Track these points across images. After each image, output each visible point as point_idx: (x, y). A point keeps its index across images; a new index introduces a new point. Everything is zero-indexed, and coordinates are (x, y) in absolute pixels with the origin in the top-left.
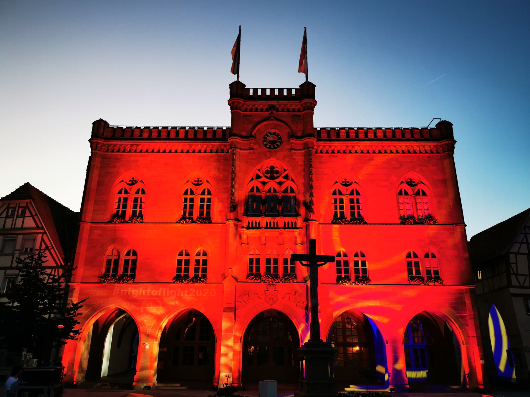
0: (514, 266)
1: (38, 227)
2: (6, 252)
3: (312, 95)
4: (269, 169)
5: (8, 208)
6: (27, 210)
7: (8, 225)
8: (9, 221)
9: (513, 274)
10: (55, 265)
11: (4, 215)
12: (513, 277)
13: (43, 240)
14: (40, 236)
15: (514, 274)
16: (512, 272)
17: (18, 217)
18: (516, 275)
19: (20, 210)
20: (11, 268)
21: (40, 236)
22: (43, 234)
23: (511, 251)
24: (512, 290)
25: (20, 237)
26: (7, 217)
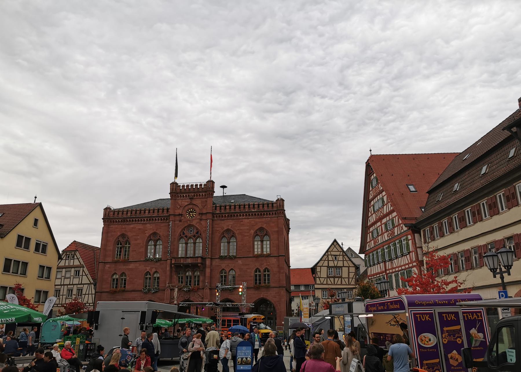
0: (319, 273)
2: (66, 276)
3: (213, 188)
5: (66, 255)
7: (67, 264)
8: (67, 261)
11: (64, 258)
12: (318, 279)
13: (83, 270)
18: (319, 278)
20: (70, 285)
24: (316, 286)
26: (66, 260)
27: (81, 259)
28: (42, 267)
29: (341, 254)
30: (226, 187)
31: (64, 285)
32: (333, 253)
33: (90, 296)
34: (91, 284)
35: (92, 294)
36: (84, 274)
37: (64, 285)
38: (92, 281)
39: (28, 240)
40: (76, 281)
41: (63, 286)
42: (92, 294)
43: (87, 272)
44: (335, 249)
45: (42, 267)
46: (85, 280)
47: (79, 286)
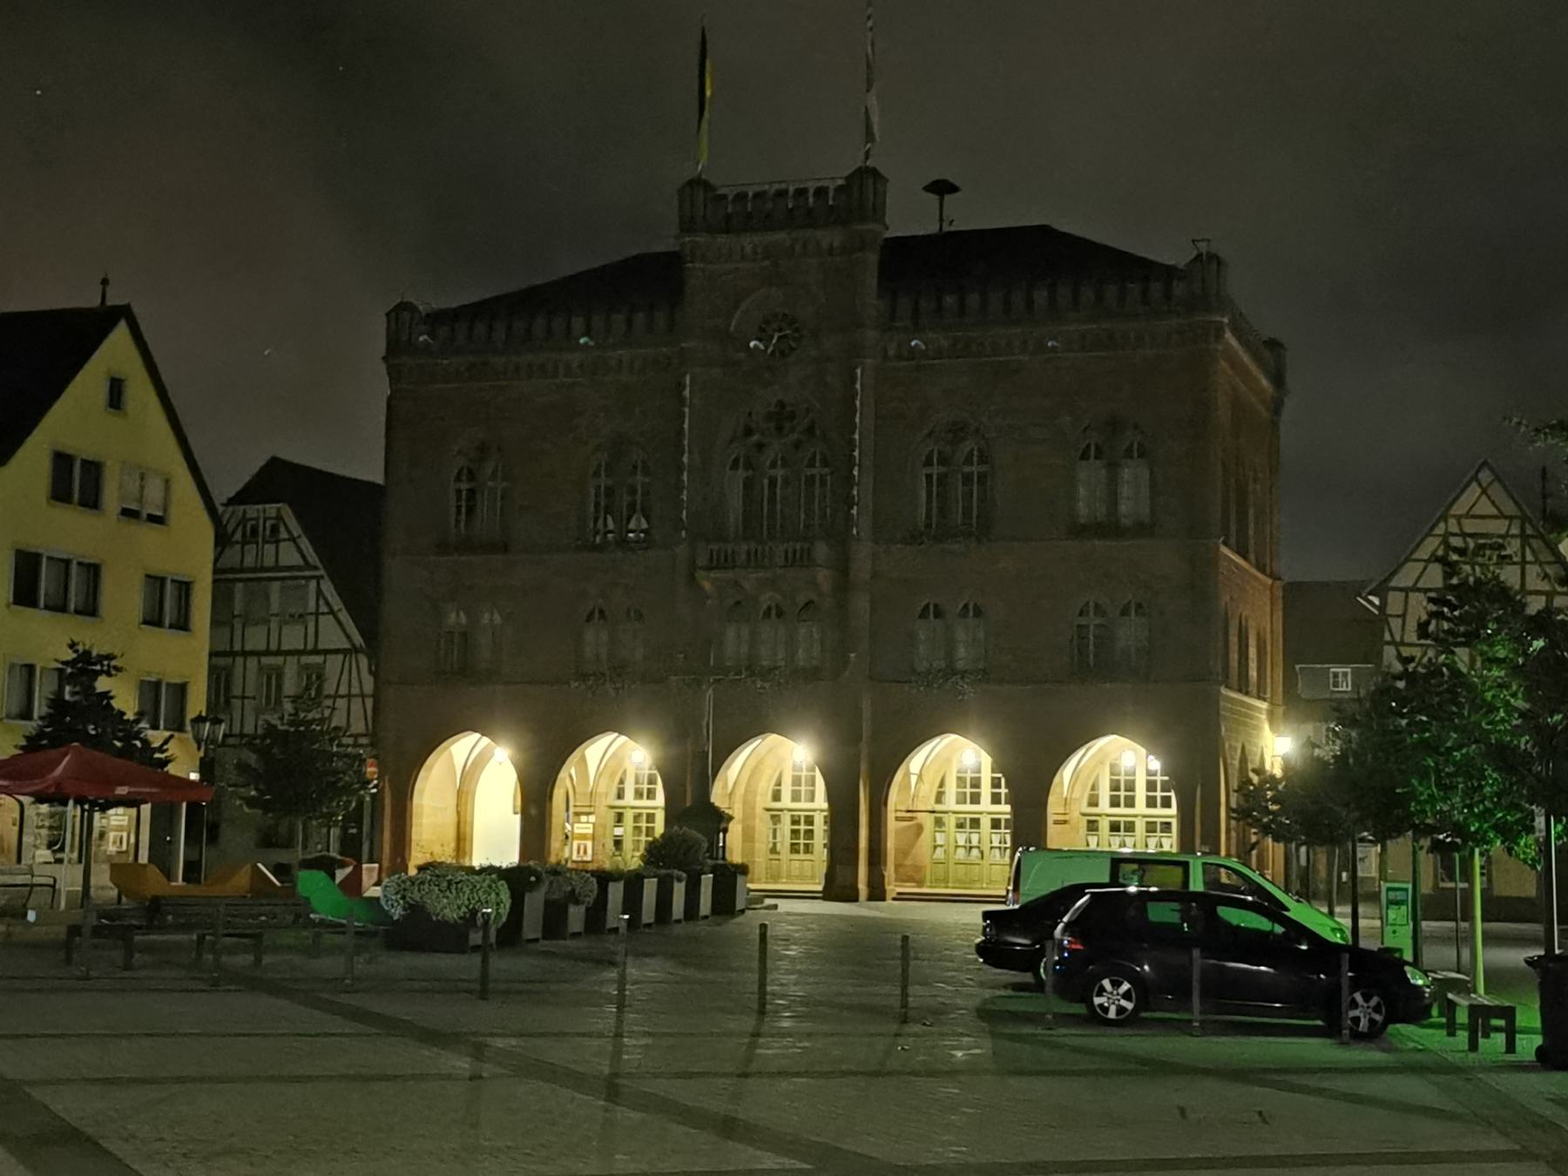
1: (308, 566)
4: (772, 409)
6: (282, 529)
9: (1388, 643)
10: (347, 646)
13: (319, 593)
14: (313, 584)
15: (1393, 643)
16: (1387, 637)
17: (265, 542)
19: (268, 524)
20: (267, 653)
21: (313, 584)
22: (319, 578)
23: (1393, 584)
25: (276, 585)
27: (305, 543)
28: (156, 583)
29: (1515, 531)
30: (953, 189)
31: (245, 654)
32: (1470, 526)
33: (356, 705)
34: (355, 650)
35: (363, 696)
36: (324, 609)
37: (245, 654)
38: (358, 639)
39: (93, 470)
40: (293, 638)
41: (239, 660)
42: (363, 696)
43: (337, 604)
44: (1485, 507)
45: (156, 583)
46: (331, 636)
47: (305, 659)
